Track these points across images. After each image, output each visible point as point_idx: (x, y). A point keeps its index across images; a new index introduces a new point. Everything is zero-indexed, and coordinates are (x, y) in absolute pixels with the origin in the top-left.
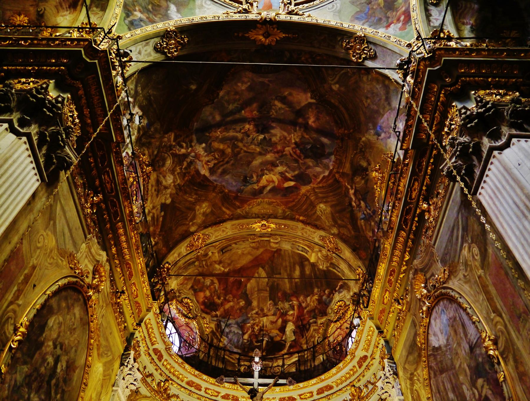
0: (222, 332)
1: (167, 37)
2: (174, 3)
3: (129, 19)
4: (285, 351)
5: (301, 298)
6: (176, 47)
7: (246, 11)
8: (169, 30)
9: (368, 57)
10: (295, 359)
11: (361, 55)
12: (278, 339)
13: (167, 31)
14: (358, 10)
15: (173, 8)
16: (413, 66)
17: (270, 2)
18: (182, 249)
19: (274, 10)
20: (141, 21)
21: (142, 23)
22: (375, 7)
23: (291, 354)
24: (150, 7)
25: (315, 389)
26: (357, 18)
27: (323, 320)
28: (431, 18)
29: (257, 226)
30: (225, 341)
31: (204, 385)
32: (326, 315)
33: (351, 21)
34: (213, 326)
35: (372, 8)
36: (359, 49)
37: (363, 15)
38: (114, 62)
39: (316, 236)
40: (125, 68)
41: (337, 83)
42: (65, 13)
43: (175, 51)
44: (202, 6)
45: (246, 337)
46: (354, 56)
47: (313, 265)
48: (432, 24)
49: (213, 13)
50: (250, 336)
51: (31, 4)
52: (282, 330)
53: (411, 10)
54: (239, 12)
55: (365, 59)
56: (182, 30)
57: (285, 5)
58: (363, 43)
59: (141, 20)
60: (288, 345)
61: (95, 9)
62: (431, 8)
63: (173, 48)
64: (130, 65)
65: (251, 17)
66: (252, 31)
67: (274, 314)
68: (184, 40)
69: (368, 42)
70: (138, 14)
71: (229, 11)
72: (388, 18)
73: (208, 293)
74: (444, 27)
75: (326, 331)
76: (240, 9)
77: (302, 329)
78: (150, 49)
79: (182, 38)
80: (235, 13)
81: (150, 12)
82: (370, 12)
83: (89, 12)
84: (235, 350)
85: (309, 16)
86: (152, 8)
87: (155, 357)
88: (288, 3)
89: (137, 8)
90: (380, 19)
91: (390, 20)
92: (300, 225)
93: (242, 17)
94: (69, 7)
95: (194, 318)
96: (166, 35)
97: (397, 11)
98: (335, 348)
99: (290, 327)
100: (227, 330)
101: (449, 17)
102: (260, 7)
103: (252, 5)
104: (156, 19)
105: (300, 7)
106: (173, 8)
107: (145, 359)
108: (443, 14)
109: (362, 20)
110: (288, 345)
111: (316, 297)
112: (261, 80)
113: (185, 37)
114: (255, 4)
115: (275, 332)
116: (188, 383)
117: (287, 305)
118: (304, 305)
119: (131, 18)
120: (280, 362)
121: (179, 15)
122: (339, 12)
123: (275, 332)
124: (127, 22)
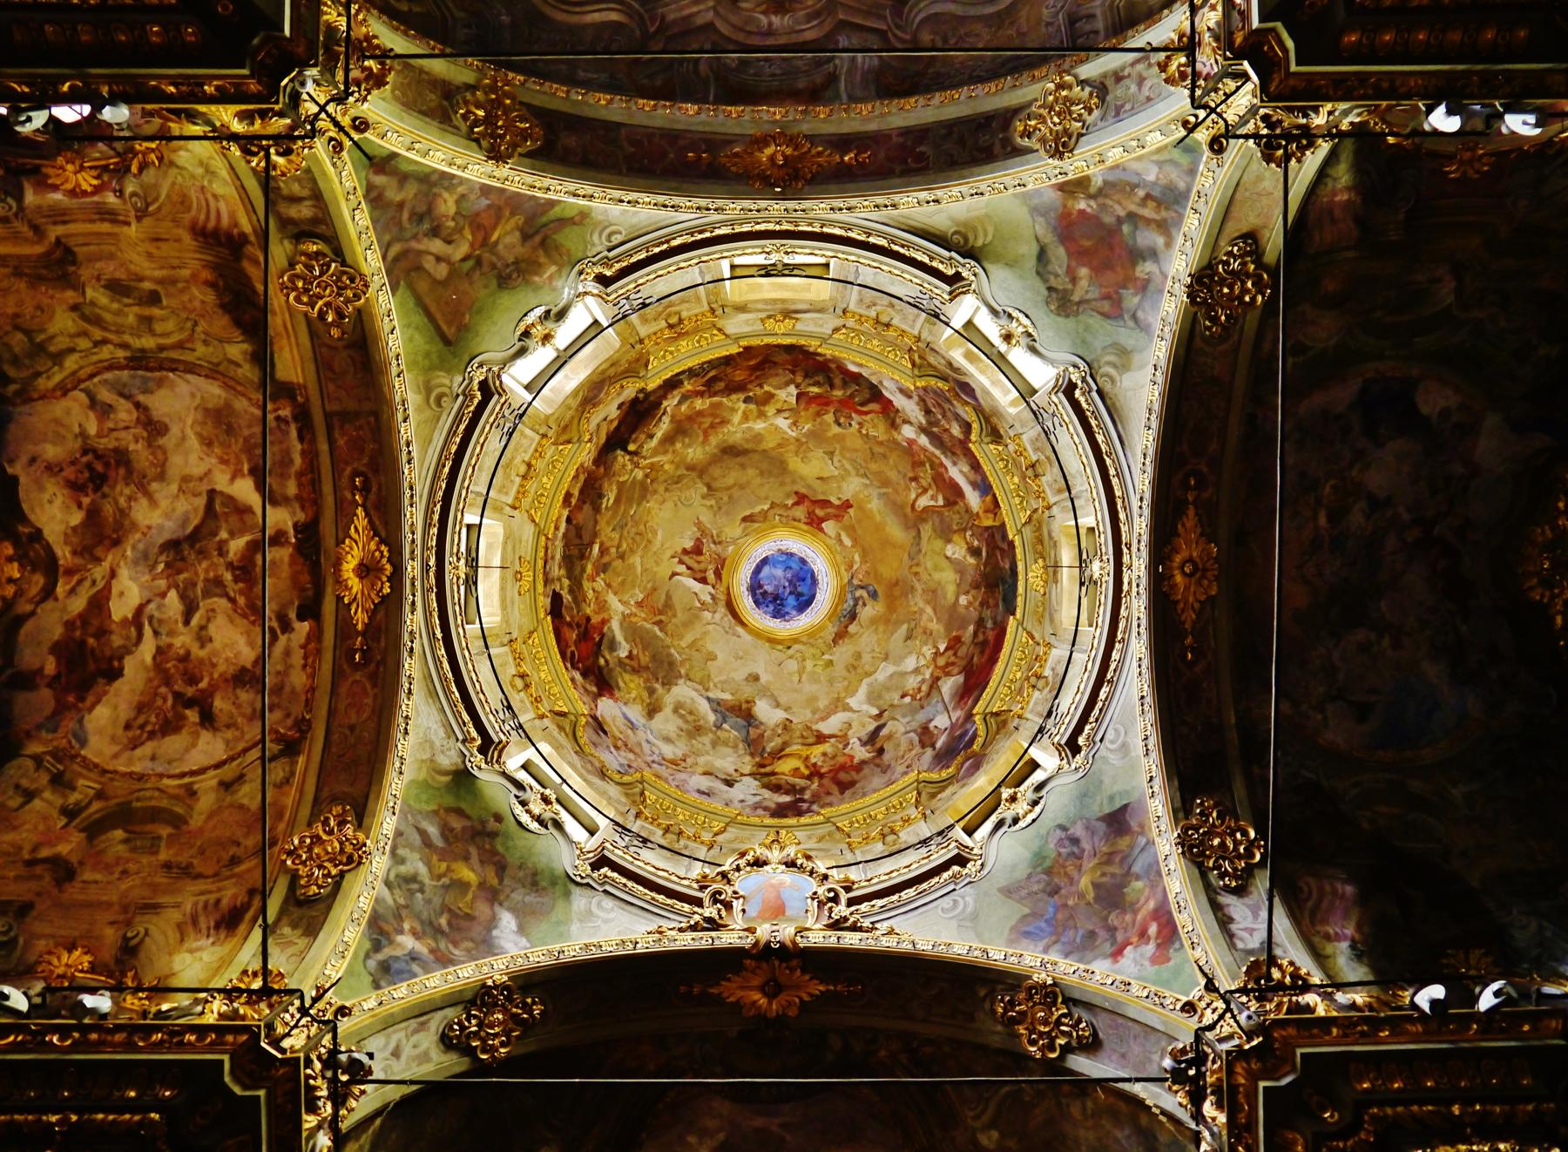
1: (484, 1004)
2: (509, 909)
3: (380, 957)
6: (507, 1033)
7: (713, 925)
8: (490, 983)
9: (1074, 1043)
11: (1053, 1040)
13: (484, 985)
14: (1027, 911)
15: (507, 921)
16: (1213, 1072)
17: (779, 897)
19: (790, 920)
20: (413, 959)
21: (415, 968)
22: (1070, 903)
24: (443, 921)
26: (1027, 934)
28: (1233, 927)
33: (1011, 943)
35: (1065, 905)
36: (1046, 1023)
37: (1043, 925)
38: (316, 1088)
40: (343, 1103)
41: (993, 1124)
42: (203, 942)
43: (503, 1044)
44: (590, 912)
46: (1033, 1043)
48: (1240, 945)
49: (619, 933)
51: (112, 918)
53: (1174, 907)
54: (694, 928)
55: (1067, 1050)
56: (529, 982)
57: (821, 904)
58: (1054, 1003)
59: (413, 957)
61: (287, 930)
62: (1226, 899)
63: (496, 1035)
64: (363, 1092)
65: (726, 939)
66: (729, 980)
68: (530, 1012)
69: (1067, 1001)
70: (407, 942)
71: (665, 924)
72: (1112, 930)
74: (1278, 952)
76: (697, 918)
78: (428, 1040)
79: (527, 1008)
80: (681, 930)
81: (442, 933)
82: (1060, 916)
83: (270, 941)
85: (891, 932)
86: (449, 923)
88: (830, 900)
89: (406, 926)
90: (1092, 935)
91: (1120, 937)
93: (703, 941)
94: (217, 927)
96: (480, 998)
97: (1135, 912)
101: (1282, 923)
102: (752, 912)
103: (728, 906)
104: (456, 952)
105: (864, 907)
106: (507, 921)
108: (1264, 914)
109: (1042, 939)
112: (759, 1122)
113: (534, 1003)
114: (737, 905)
119: (387, 952)
121: (524, 942)
122: (974, 917)
124: (372, 964)
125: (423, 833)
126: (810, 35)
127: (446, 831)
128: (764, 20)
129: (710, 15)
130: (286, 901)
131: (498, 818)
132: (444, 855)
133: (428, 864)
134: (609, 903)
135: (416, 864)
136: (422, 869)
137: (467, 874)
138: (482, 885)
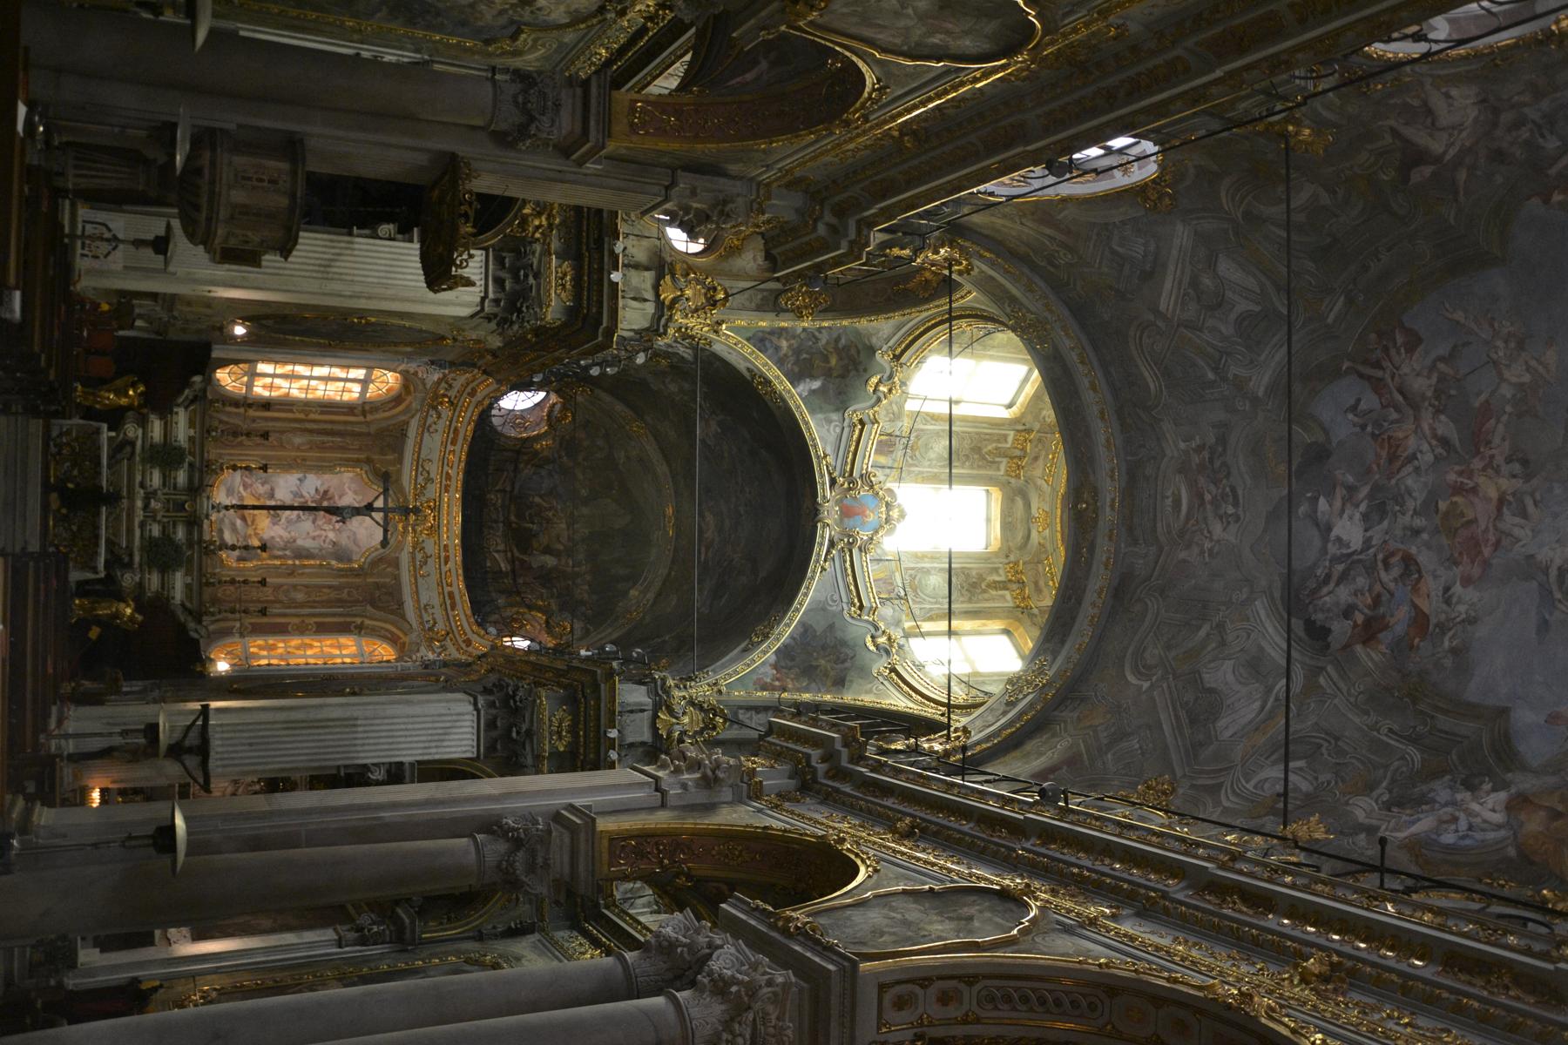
0: (541, 467)
4: (517, 554)
5: (588, 578)
10: (504, 566)
12: (535, 545)
15: (816, 385)
18: (619, 407)
23: (512, 561)
25: (454, 589)
26: (806, 631)
27: (554, 607)
29: (670, 511)
30: (527, 471)
31: (457, 448)
32: (561, 610)
34: (546, 453)
39: (651, 595)
45: (537, 499)
47: (625, 594)
50: (538, 505)
52: (548, 550)
59: (777, 348)
60: (525, 558)
67: (569, 539)
73: (586, 443)
75: (539, 609)
77: (546, 578)
84: (517, 487)
87: (469, 390)
92: (665, 572)
95: (550, 426)
98: (516, 620)
99: (550, 561)
100: (543, 473)
106: (816, 385)
107: (462, 379)
110: (525, 558)
111: (586, 596)
115: (544, 540)
116: (456, 430)
117: (581, 556)
118: (579, 581)
120: (501, 547)
123: (544, 540)
125: (837, 340)
126: (1159, 525)
127: (846, 348)
128: (1169, 493)
129: (1168, 452)
130: (771, 291)
131: (865, 370)
132: (836, 349)
133: (828, 343)
134: (838, 430)
135: (824, 338)
136: (824, 341)
137: (833, 361)
138: (830, 369)
